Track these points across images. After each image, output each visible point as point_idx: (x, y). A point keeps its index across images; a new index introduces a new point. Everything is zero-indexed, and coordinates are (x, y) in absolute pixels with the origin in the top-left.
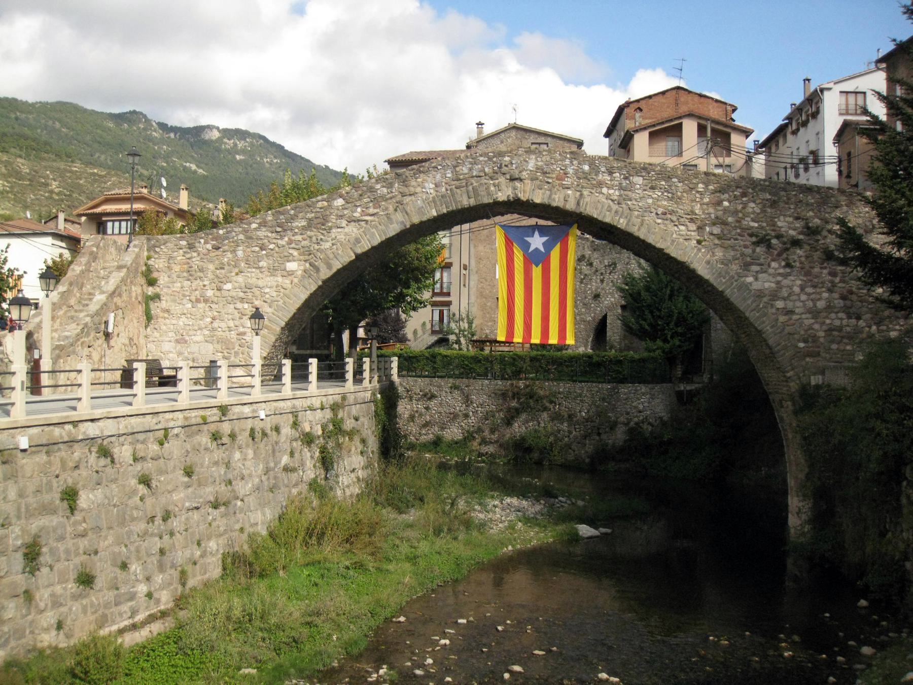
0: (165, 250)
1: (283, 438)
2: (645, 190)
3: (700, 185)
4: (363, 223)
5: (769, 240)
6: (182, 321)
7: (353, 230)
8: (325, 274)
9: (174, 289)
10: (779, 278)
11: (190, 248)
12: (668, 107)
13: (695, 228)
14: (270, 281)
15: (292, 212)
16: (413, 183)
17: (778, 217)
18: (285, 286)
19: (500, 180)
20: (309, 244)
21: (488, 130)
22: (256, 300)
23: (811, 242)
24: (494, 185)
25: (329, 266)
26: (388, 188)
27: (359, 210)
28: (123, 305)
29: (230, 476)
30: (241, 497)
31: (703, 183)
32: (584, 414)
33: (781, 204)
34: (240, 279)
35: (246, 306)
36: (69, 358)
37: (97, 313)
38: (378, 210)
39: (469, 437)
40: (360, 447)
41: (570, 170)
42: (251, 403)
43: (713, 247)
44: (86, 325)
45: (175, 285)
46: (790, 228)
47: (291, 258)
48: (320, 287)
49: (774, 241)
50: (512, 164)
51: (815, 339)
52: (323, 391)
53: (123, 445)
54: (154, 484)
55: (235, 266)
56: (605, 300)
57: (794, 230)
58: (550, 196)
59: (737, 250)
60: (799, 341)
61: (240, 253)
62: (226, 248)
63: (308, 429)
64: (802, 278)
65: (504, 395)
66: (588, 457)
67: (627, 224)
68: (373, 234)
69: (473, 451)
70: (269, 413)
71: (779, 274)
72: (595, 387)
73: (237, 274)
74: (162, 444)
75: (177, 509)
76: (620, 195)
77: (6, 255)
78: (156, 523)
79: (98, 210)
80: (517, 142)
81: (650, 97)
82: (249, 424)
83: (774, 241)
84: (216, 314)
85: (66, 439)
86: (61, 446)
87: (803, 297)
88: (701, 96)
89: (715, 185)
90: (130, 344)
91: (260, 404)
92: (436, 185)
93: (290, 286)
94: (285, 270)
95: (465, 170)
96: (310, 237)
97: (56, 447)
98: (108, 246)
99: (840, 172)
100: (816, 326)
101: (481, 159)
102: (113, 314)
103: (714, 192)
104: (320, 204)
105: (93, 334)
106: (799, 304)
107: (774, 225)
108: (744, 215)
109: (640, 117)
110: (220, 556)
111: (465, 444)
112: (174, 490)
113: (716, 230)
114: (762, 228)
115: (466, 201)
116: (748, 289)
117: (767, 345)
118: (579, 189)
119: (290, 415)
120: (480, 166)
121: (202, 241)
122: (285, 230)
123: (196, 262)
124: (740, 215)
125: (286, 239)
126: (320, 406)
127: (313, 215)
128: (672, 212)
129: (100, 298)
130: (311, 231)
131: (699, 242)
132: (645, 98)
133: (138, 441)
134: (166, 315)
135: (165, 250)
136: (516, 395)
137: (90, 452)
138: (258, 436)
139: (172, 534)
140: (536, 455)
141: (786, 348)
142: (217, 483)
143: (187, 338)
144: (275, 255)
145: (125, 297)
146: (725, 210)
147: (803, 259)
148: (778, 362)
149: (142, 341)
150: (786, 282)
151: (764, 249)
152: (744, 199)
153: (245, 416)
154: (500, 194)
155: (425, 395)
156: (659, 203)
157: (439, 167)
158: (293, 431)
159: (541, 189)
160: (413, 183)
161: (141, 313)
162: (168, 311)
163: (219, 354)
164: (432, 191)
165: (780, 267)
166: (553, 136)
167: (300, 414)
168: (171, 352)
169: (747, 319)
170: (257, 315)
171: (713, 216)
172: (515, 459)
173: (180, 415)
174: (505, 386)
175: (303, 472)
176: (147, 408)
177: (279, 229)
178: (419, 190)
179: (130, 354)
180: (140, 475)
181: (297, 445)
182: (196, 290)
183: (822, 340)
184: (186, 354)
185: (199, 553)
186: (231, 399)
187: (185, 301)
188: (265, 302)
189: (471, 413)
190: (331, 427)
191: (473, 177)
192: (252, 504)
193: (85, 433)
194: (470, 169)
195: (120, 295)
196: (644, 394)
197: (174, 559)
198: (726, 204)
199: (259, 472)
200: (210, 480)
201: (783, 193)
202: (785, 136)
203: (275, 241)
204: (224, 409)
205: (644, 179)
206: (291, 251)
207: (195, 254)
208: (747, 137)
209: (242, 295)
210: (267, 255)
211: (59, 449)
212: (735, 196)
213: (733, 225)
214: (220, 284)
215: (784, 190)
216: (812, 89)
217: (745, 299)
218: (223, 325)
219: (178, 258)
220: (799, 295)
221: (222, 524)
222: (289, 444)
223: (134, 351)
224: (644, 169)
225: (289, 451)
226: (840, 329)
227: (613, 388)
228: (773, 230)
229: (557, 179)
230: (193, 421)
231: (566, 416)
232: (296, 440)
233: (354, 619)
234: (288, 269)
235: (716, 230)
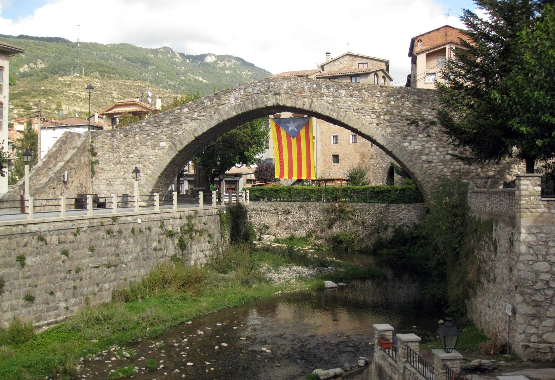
0: (100, 138)
1: (153, 234)
2: (347, 97)
3: (378, 93)
4: (198, 121)
5: (417, 122)
6: (110, 174)
7: (193, 124)
8: (180, 148)
10: (424, 143)
11: (113, 137)
12: (441, 38)
15: (163, 116)
16: (224, 98)
17: (422, 109)
18: (159, 155)
19: (269, 95)
20: (171, 132)
21: (334, 56)
25: (182, 144)
27: (196, 113)
28: (75, 167)
29: (118, 252)
30: (125, 262)
31: (379, 92)
32: (370, 221)
33: (424, 102)
34: (137, 152)
35: (141, 165)
36: (42, 194)
37: (58, 172)
38: (206, 113)
39: (309, 235)
40: (208, 239)
41: (306, 88)
42: (133, 215)
43: (385, 127)
44: (51, 178)
45: (106, 155)
46: (429, 115)
47: (162, 140)
49: (420, 123)
50: (275, 86)
52: (182, 209)
53: (52, 235)
54: (70, 255)
55: (135, 145)
57: (432, 116)
58: (295, 103)
61: (137, 138)
63: (170, 228)
64: (436, 142)
65: (327, 211)
66: (373, 246)
67: (337, 116)
68: (204, 126)
69: (312, 243)
70: (144, 220)
72: (377, 206)
73: (136, 149)
74: (75, 235)
75: (84, 267)
76: (333, 101)
77: (3, 145)
78: (72, 274)
81: (430, 32)
82: (131, 226)
83: (420, 123)
84: (126, 170)
85: (20, 232)
86: (17, 236)
87: (437, 154)
89: (386, 93)
90: (81, 186)
91: (138, 216)
92: (236, 99)
93: (162, 155)
94: (159, 146)
95: (250, 90)
96: (172, 129)
97: (14, 236)
100: (446, 170)
101: (259, 84)
103: (386, 96)
104: (176, 112)
105: (56, 182)
106: (435, 157)
107: (420, 114)
108: (403, 109)
109: (421, 45)
110: (111, 291)
111: (307, 239)
113: (387, 117)
114: (413, 115)
115: (251, 107)
116: (406, 149)
117: (418, 181)
118: (311, 97)
119: (159, 222)
120: (258, 88)
121: (118, 132)
122: (159, 126)
123: (115, 143)
124: (401, 109)
125: (160, 130)
126: (179, 217)
129: (61, 164)
131: (378, 124)
132: (427, 33)
133: (61, 234)
134: (102, 171)
135: (100, 138)
136: (334, 211)
137: (33, 238)
138: (137, 232)
139: (81, 279)
140: (344, 245)
141: (428, 182)
142: (110, 255)
143: (112, 183)
144: (155, 139)
145: (76, 162)
146: (392, 106)
147: (437, 132)
149: (89, 185)
151: (414, 127)
152: (403, 100)
153: (128, 222)
154: (269, 102)
155: (285, 212)
156: (355, 104)
157: (237, 89)
158: (160, 230)
159: (290, 99)
160: (224, 98)
161: (88, 171)
162: (102, 169)
163: (128, 191)
164: (233, 102)
165: (424, 137)
167: (165, 222)
171: (385, 110)
172: (333, 248)
173: (87, 222)
174: (328, 206)
175: (167, 251)
176: (67, 218)
177: (156, 125)
178: (226, 102)
179: (81, 191)
180: (62, 250)
181: (163, 237)
182: (116, 158)
183: (449, 177)
184: (112, 191)
185: (97, 289)
186: (119, 213)
187: (111, 164)
188: (150, 163)
189: (310, 222)
190: (186, 228)
191: (254, 94)
192: (132, 267)
193: (30, 229)
194: (253, 90)
195: (73, 162)
196: (403, 209)
197: (82, 291)
198: (392, 103)
199: (138, 250)
200: (106, 254)
201: (424, 96)
203: (154, 131)
204: (114, 219)
205: (346, 91)
206: (162, 136)
207: (115, 140)
209: (138, 160)
210: (150, 139)
211: (15, 237)
213: (396, 114)
215: (425, 93)
217: (404, 155)
220: (435, 152)
221: (112, 276)
222: (157, 236)
225: (158, 240)
227: (386, 206)
228: (419, 116)
229: (300, 93)
230: (95, 224)
231: (361, 223)
232: (162, 234)
233: (163, 321)
234: (161, 146)
235: (387, 117)
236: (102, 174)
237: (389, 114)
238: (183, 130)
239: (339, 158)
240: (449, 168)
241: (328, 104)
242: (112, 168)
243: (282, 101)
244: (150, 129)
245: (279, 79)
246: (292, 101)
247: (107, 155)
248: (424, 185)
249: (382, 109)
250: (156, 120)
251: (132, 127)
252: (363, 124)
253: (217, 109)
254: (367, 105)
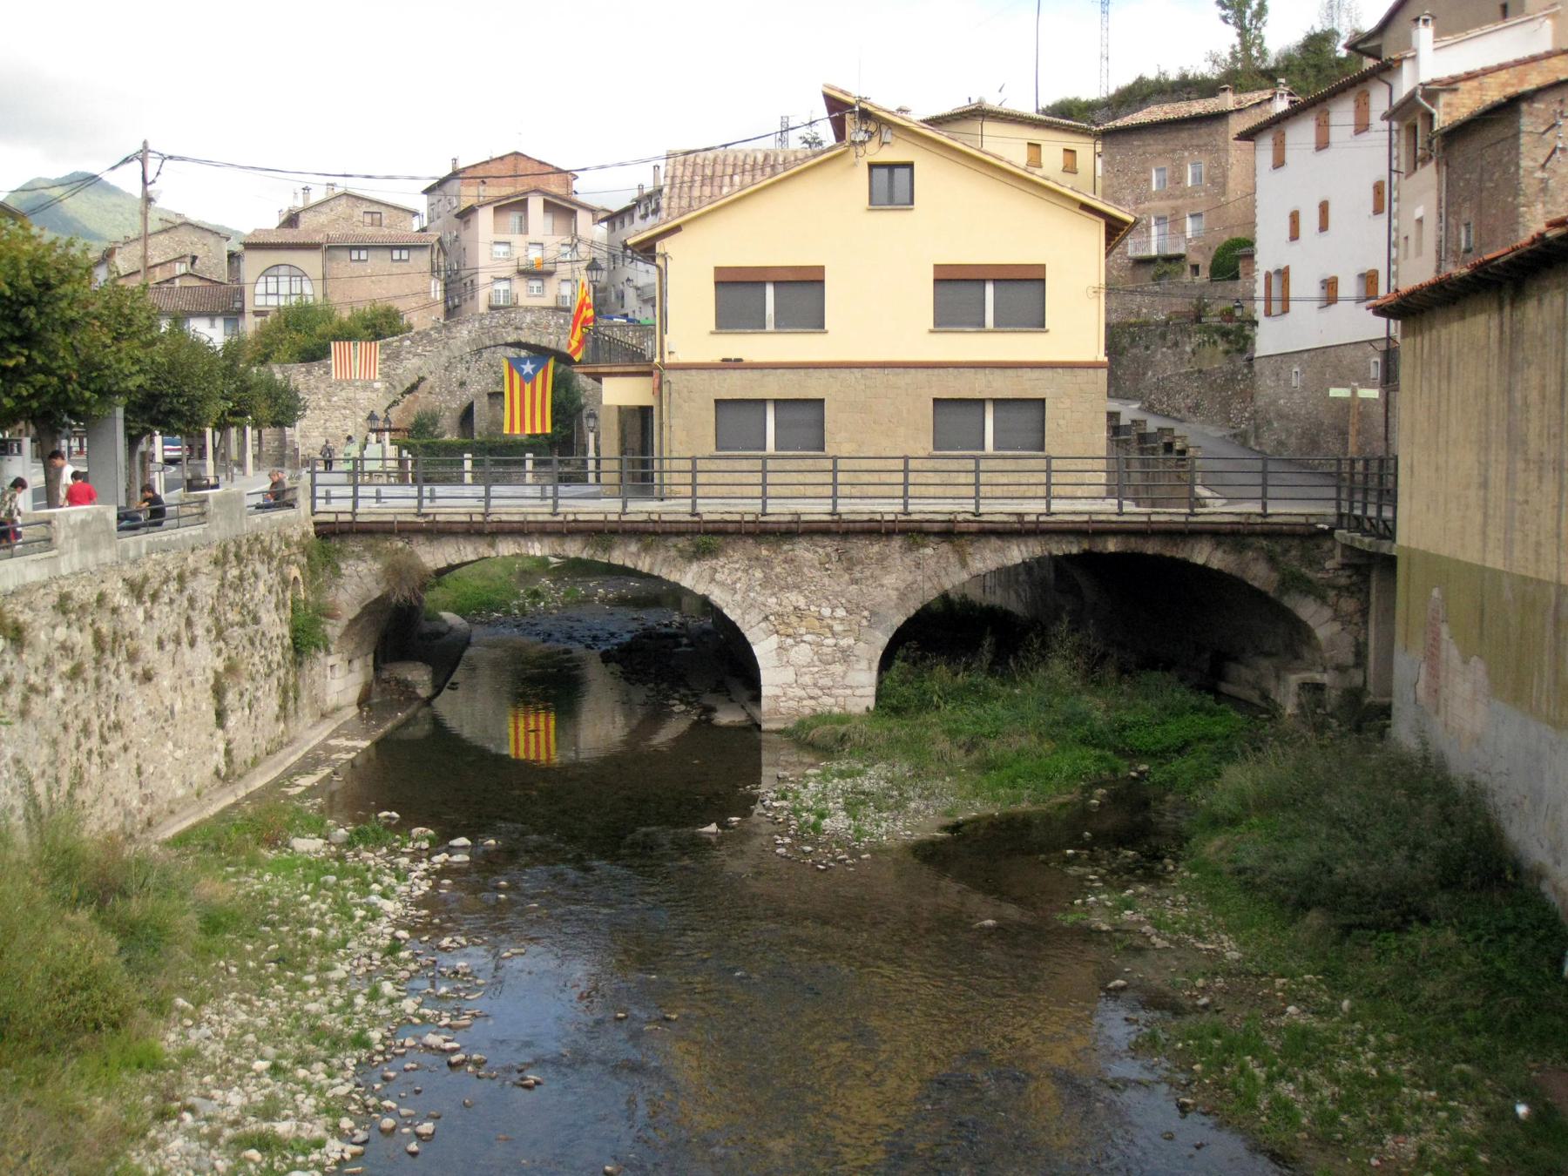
7: (416, 361)
16: (454, 330)
25: (402, 386)
34: (343, 393)
80: (348, 211)
88: (541, 163)
123: (312, 382)
166: (387, 205)
202: (632, 216)
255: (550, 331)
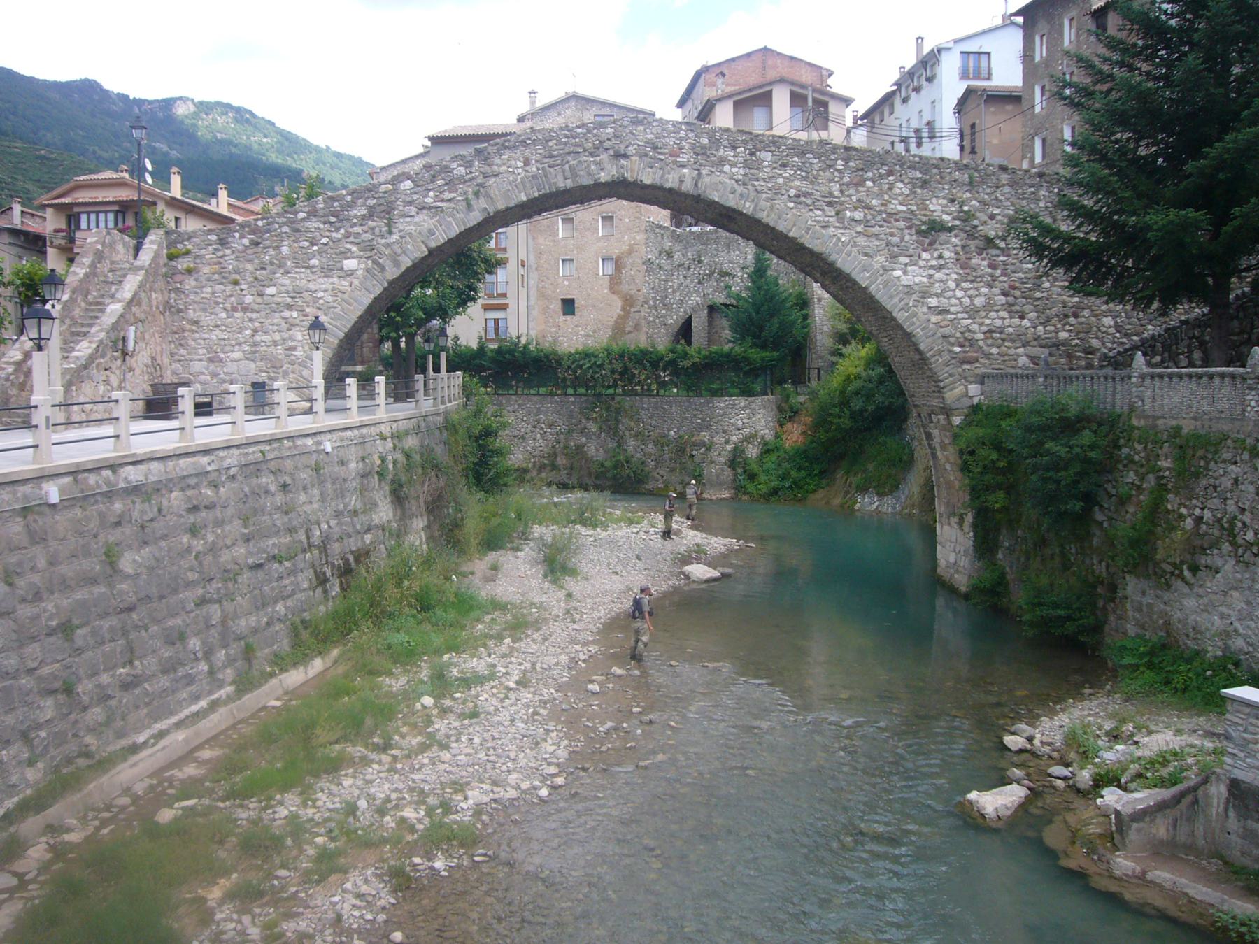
2: (775, 168)
7: (424, 221)
8: (392, 273)
9: (203, 295)
10: (932, 272)
11: (222, 245)
13: (833, 213)
14: (325, 283)
17: (930, 199)
18: (342, 288)
19: (602, 157)
20: (371, 237)
21: (542, 101)
22: (308, 306)
23: (968, 228)
24: (596, 163)
25: (397, 264)
26: (466, 167)
27: (431, 194)
28: (143, 316)
31: (842, 159)
35: (295, 314)
45: (204, 290)
47: (349, 255)
48: (385, 289)
51: (972, 342)
55: (280, 266)
56: (690, 299)
58: (662, 176)
59: (882, 240)
60: (953, 345)
62: (267, 243)
67: (754, 209)
71: (932, 267)
76: (745, 175)
79: (67, 200)
81: (733, 60)
87: (959, 294)
88: (792, 58)
92: (527, 162)
94: (342, 269)
96: (373, 229)
98: (114, 242)
99: (962, 148)
100: (975, 327)
101: (579, 130)
102: (133, 328)
109: (723, 83)
112: (233, 544)
113: (859, 215)
114: (912, 212)
121: (237, 235)
123: (230, 263)
124: (886, 197)
127: (375, 201)
128: (806, 195)
129: (114, 309)
130: (373, 221)
133: (189, 486)
134: (194, 328)
141: (939, 353)
143: (222, 355)
147: (959, 249)
148: (930, 369)
150: (938, 276)
152: (891, 178)
154: (603, 174)
157: (528, 142)
159: (651, 167)
160: (497, 161)
162: (197, 323)
163: (264, 374)
168: (203, 373)
169: (894, 319)
170: (316, 325)
171: (854, 199)
173: (235, 452)
177: (333, 219)
178: (504, 168)
182: (231, 296)
183: (981, 343)
184: (222, 376)
187: (217, 310)
188: (319, 309)
195: (139, 304)
198: (869, 183)
201: (935, 171)
202: (892, 105)
203: (328, 234)
206: (348, 246)
207: (228, 252)
208: (847, 106)
209: (289, 300)
210: (320, 252)
211: (96, 502)
212: (880, 175)
213: (878, 209)
214: (261, 288)
215: (937, 167)
216: (926, 50)
217: (891, 297)
218: (267, 338)
219: (207, 257)
220: (954, 290)
223: (159, 373)
224: (774, 143)
226: (1001, 330)
228: (924, 215)
229: (671, 156)
230: (251, 458)
234: (345, 268)
235: (859, 215)
236: (197, 335)
237: (864, 208)
238: (400, 231)
239: (576, 305)
240: (981, 324)
241: (733, 182)
242: (221, 319)
243: (632, 170)
244: (319, 228)
245: (626, 123)
246: (654, 173)
247: (209, 290)
248: (933, 360)
249: (849, 196)
250: (333, 207)
251: (272, 223)
252: (808, 229)
253: (482, 185)
254: (818, 188)
255: (682, 159)
